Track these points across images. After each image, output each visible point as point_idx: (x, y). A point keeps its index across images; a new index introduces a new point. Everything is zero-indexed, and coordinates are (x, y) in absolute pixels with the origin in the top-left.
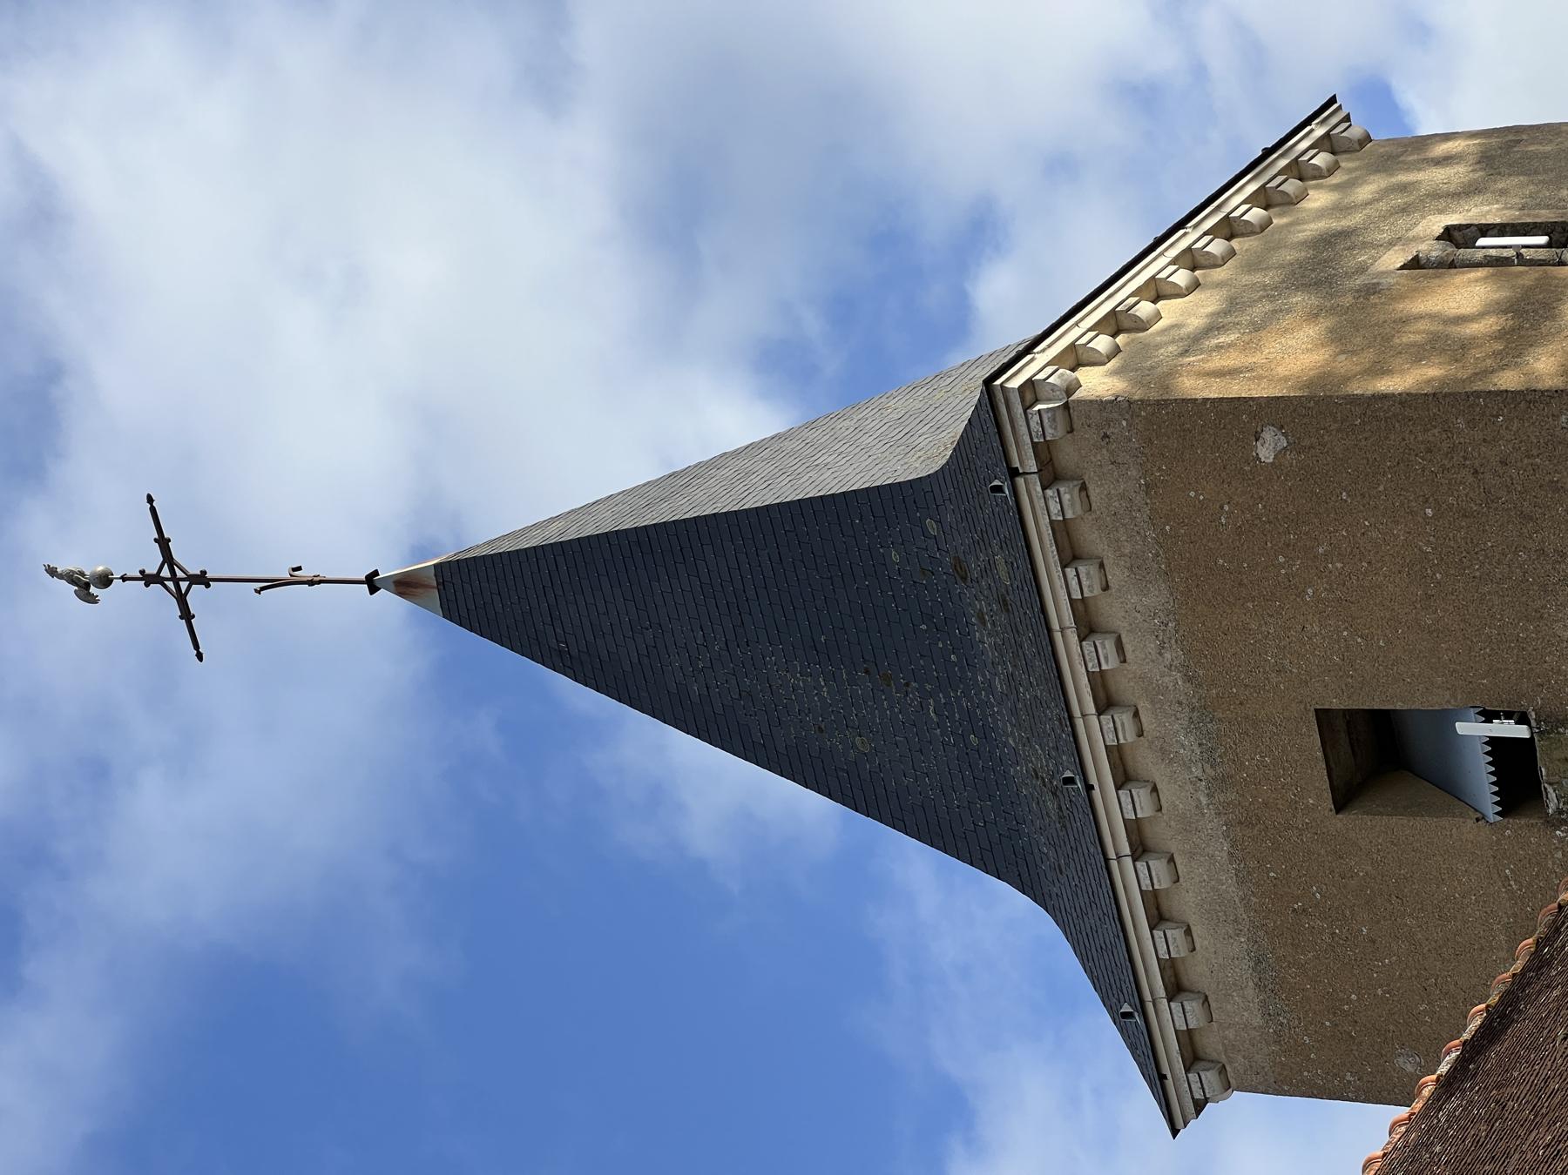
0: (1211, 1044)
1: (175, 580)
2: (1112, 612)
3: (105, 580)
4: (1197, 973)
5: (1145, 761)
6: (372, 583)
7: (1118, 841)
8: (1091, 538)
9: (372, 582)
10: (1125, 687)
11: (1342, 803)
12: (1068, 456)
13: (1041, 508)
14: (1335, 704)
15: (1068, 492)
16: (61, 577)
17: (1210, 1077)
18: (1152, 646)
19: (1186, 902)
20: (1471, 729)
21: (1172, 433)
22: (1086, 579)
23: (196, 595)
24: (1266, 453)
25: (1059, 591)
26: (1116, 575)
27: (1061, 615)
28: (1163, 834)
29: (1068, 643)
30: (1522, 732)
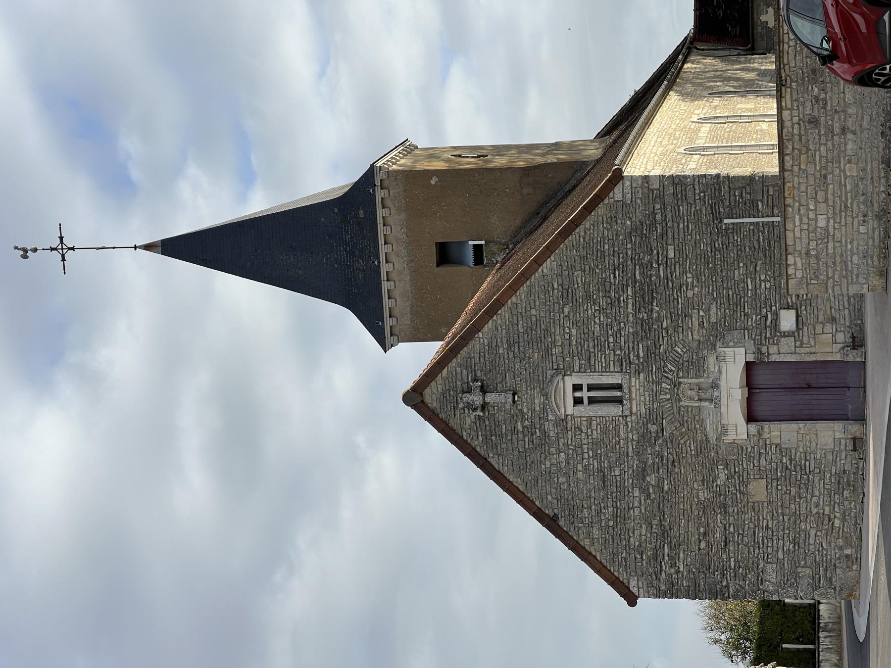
0: (396, 330)
1: (62, 249)
2: (390, 221)
3: (35, 250)
4: (396, 312)
5: (393, 258)
6: (135, 247)
7: (384, 276)
8: (388, 203)
9: (135, 247)
10: (390, 239)
11: (438, 266)
12: (386, 183)
13: (380, 194)
14: (440, 241)
15: (386, 191)
16: (20, 249)
17: (396, 338)
18: (399, 229)
19: (396, 294)
20: (471, 243)
21: (413, 179)
22: (386, 212)
23: (69, 255)
24: (433, 182)
25: (380, 213)
26: (393, 212)
27: (380, 220)
28: (393, 276)
29: (380, 226)
30: (483, 242)
